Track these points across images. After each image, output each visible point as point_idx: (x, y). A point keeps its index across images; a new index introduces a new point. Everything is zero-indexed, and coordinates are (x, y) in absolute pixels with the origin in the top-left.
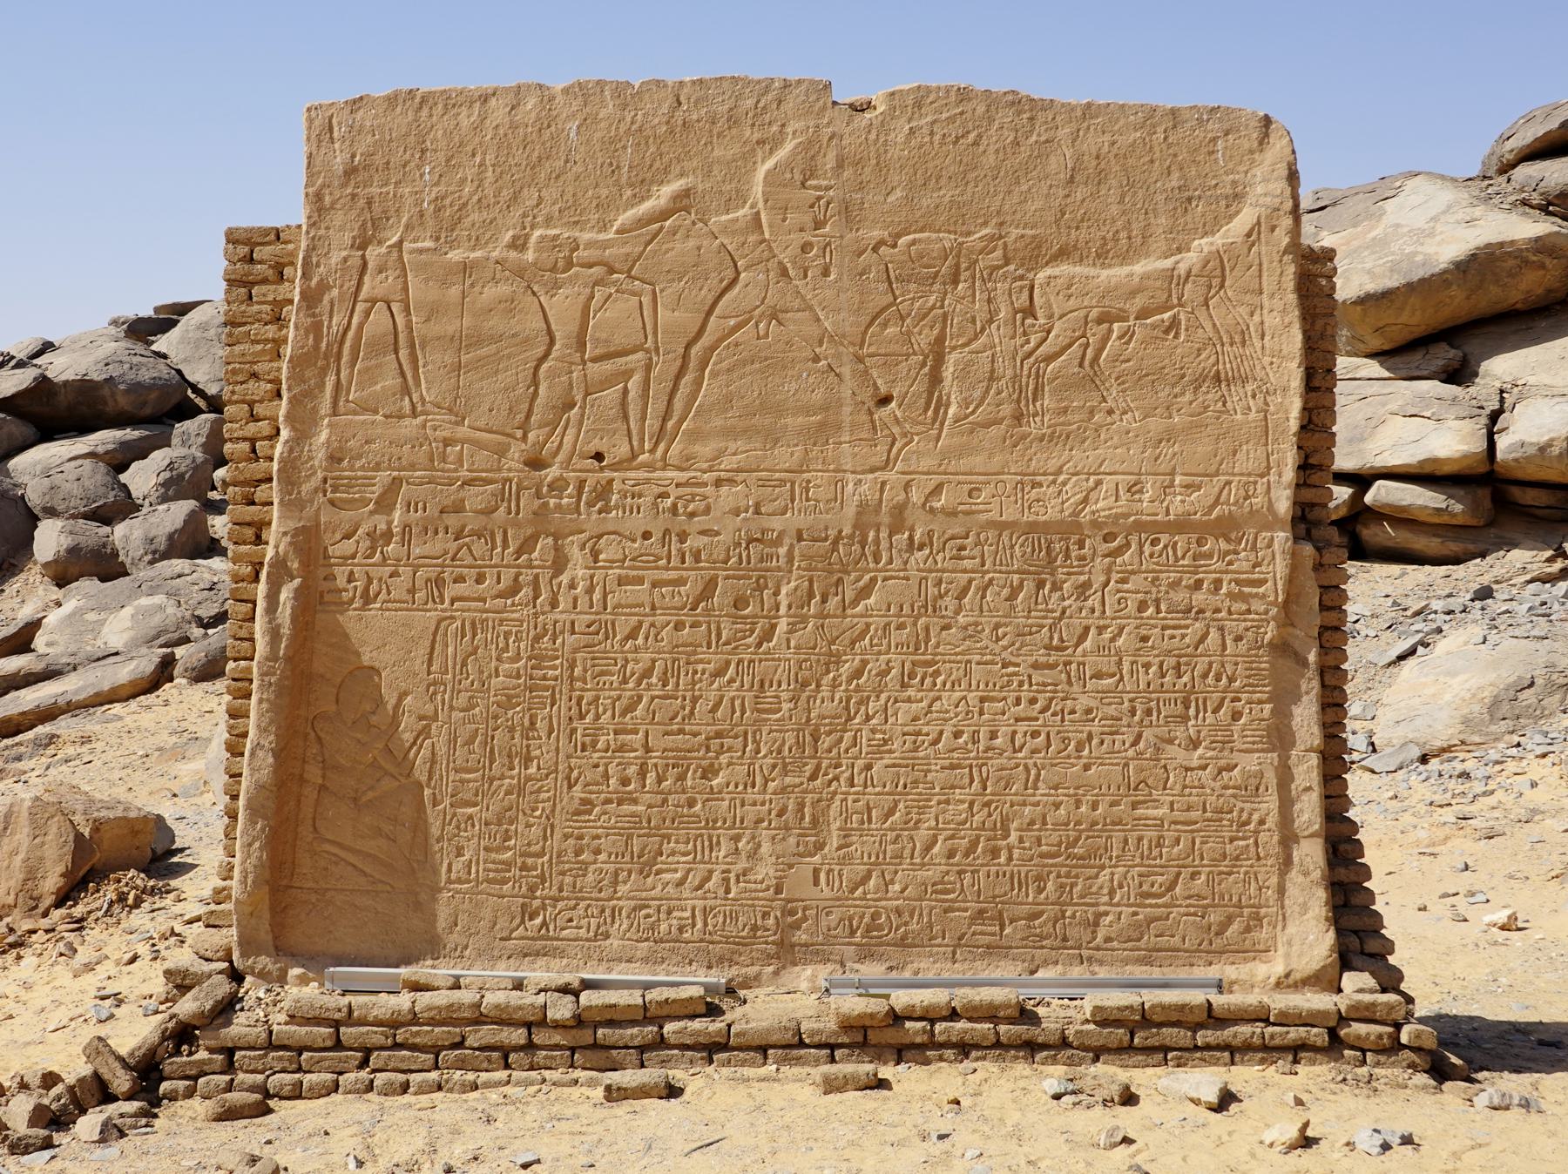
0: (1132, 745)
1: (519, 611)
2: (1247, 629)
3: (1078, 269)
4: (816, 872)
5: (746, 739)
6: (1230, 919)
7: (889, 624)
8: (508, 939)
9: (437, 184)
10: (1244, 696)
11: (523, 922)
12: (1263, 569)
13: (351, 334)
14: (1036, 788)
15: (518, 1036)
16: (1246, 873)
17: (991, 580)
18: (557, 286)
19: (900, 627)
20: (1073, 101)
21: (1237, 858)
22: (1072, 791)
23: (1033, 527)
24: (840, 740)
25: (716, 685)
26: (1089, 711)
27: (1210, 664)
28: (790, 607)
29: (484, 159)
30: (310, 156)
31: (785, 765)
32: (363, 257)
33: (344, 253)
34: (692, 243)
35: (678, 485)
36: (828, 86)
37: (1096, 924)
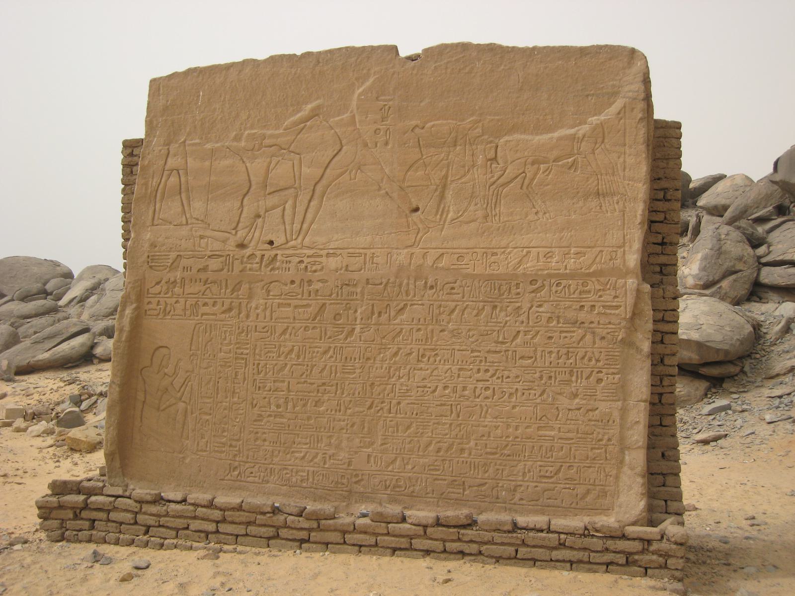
0: (540, 395)
2: (608, 333)
3: (523, 137)
6: (588, 492)
8: (223, 480)
10: (604, 370)
11: (230, 471)
13: (161, 186)
14: (485, 417)
17: (467, 305)
19: (419, 330)
21: (594, 459)
22: (505, 420)
23: (490, 278)
24: (385, 389)
26: (517, 377)
27: (586, 352)
28: (362, 319)
32: (168, 149)
33: (160, 148)
35: (308, 257)
37: (515, 490)
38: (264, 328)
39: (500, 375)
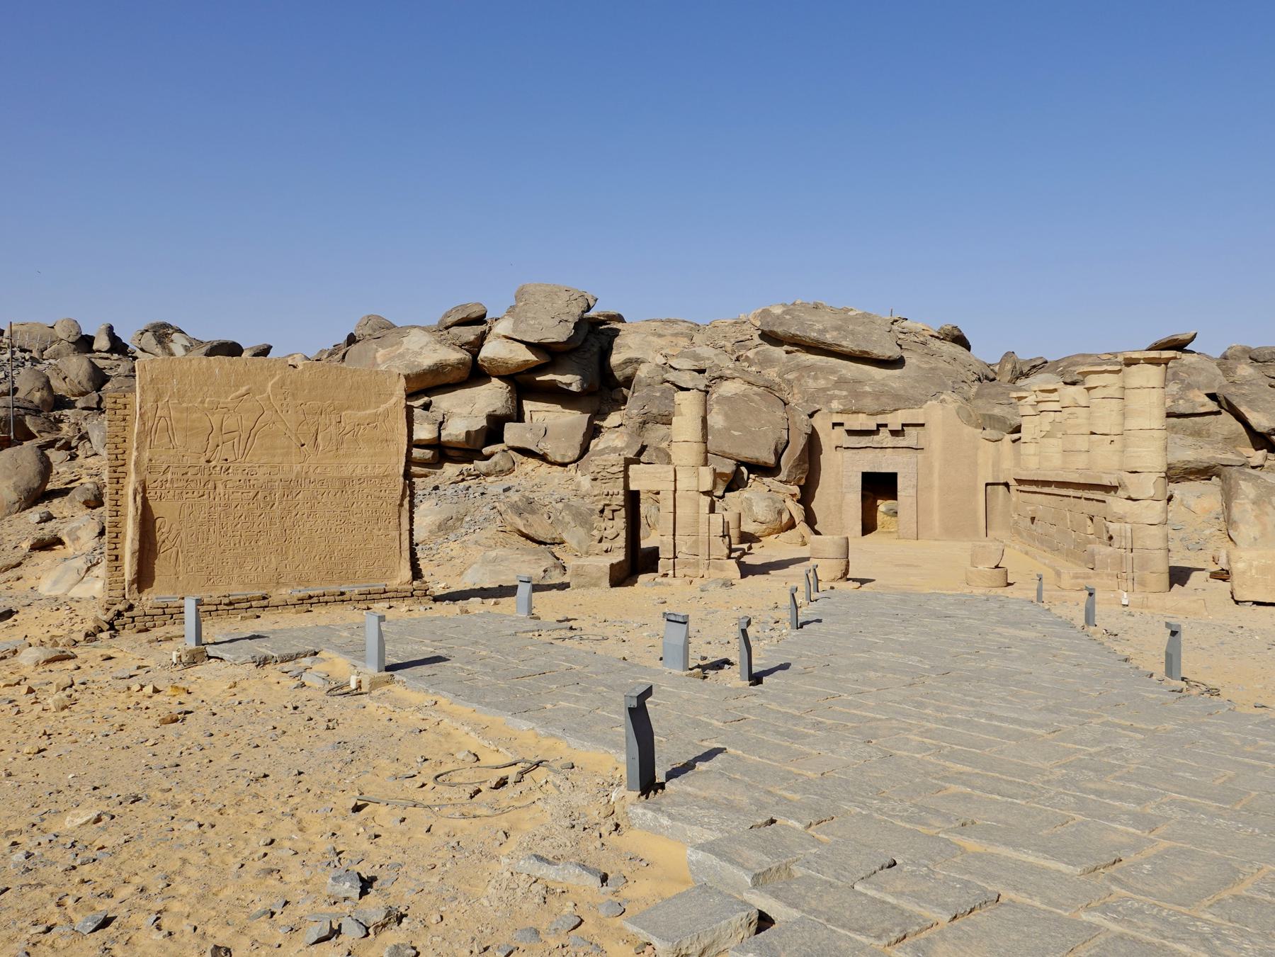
15: (214, 608)
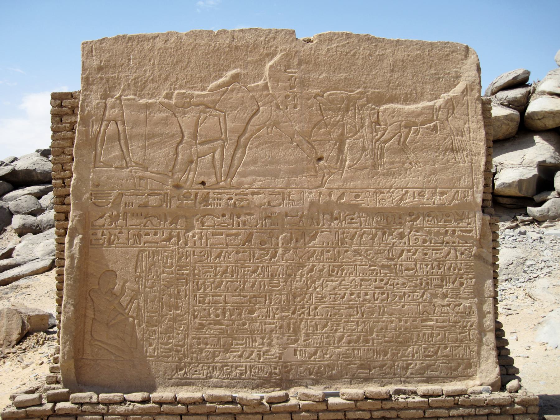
0: (422, 296)
1: (172, 246)
2: (466, 250)
4: (295, 351)
5: (266, 298)
6: (459, 364)
7: (323, 250)
9: (135, 72)
12: (471, 226)
16: (465, 346)
17: (364, 232)
18: (185, 113)
19: (328, 251)
20: (392, 39)
24: (304, 298)
25: (253, 276)
26: (404, 284)
27: (451, 264)
28: (283, 244)
29: (154, 62)
30: (83, 62)
31: (282, 308)
32: (105, 103)
33: (98, 101)
34: (240, 95)
35: (236, 195)
36: (294, 32)
38: (201, 253)
39: (392, 283)
